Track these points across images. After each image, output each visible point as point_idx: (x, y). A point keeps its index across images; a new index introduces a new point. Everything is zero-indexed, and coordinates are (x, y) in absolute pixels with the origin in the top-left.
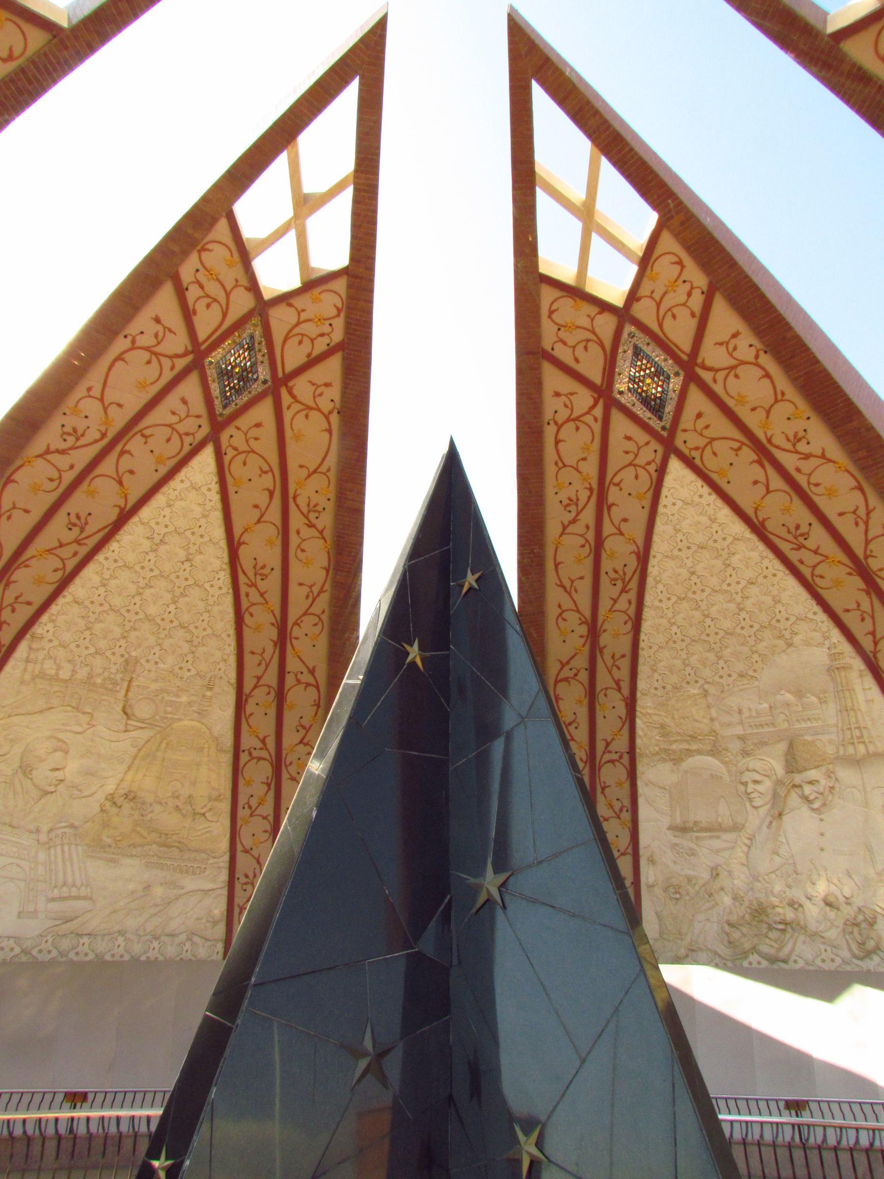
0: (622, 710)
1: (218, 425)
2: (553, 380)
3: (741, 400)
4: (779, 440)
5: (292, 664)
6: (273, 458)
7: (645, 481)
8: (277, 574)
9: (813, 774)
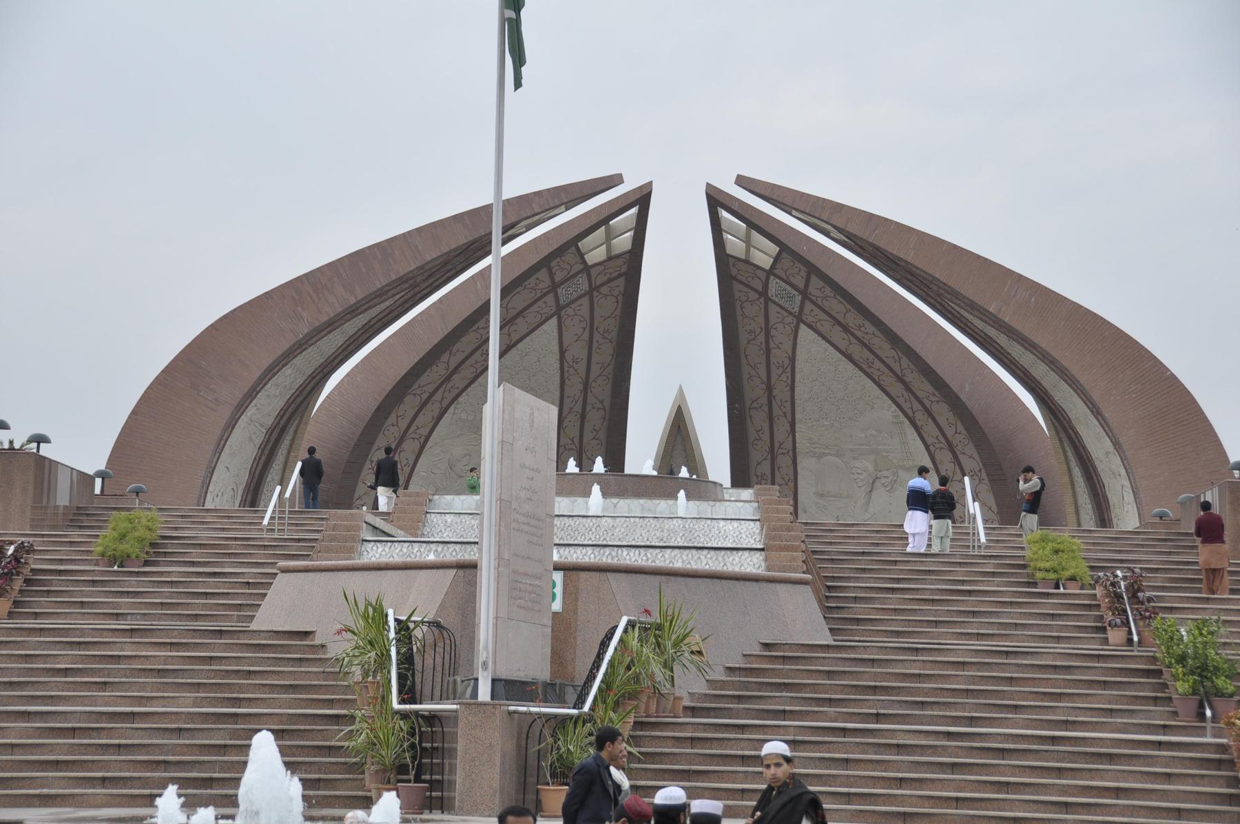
1: (559, 308)
2: (737, 286)
5: (591, 400)
8: (585, 361)
9: (885, 473)
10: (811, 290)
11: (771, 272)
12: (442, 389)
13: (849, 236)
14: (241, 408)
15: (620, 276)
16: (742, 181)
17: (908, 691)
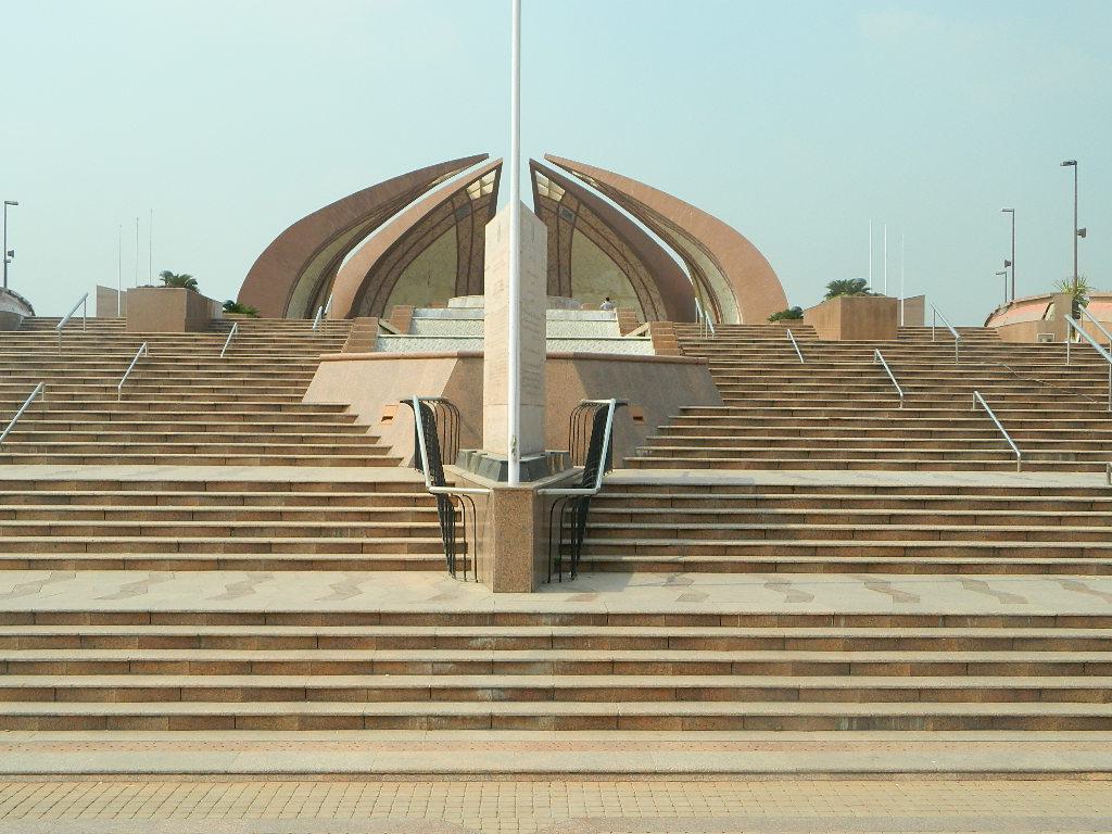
2: (544, 210)
5: (472, 267)
10: (581, 212)
11: (561, 202)
13: (601, 184)
14: (302, 271)
16: (547, 157)
17: (795, 443)
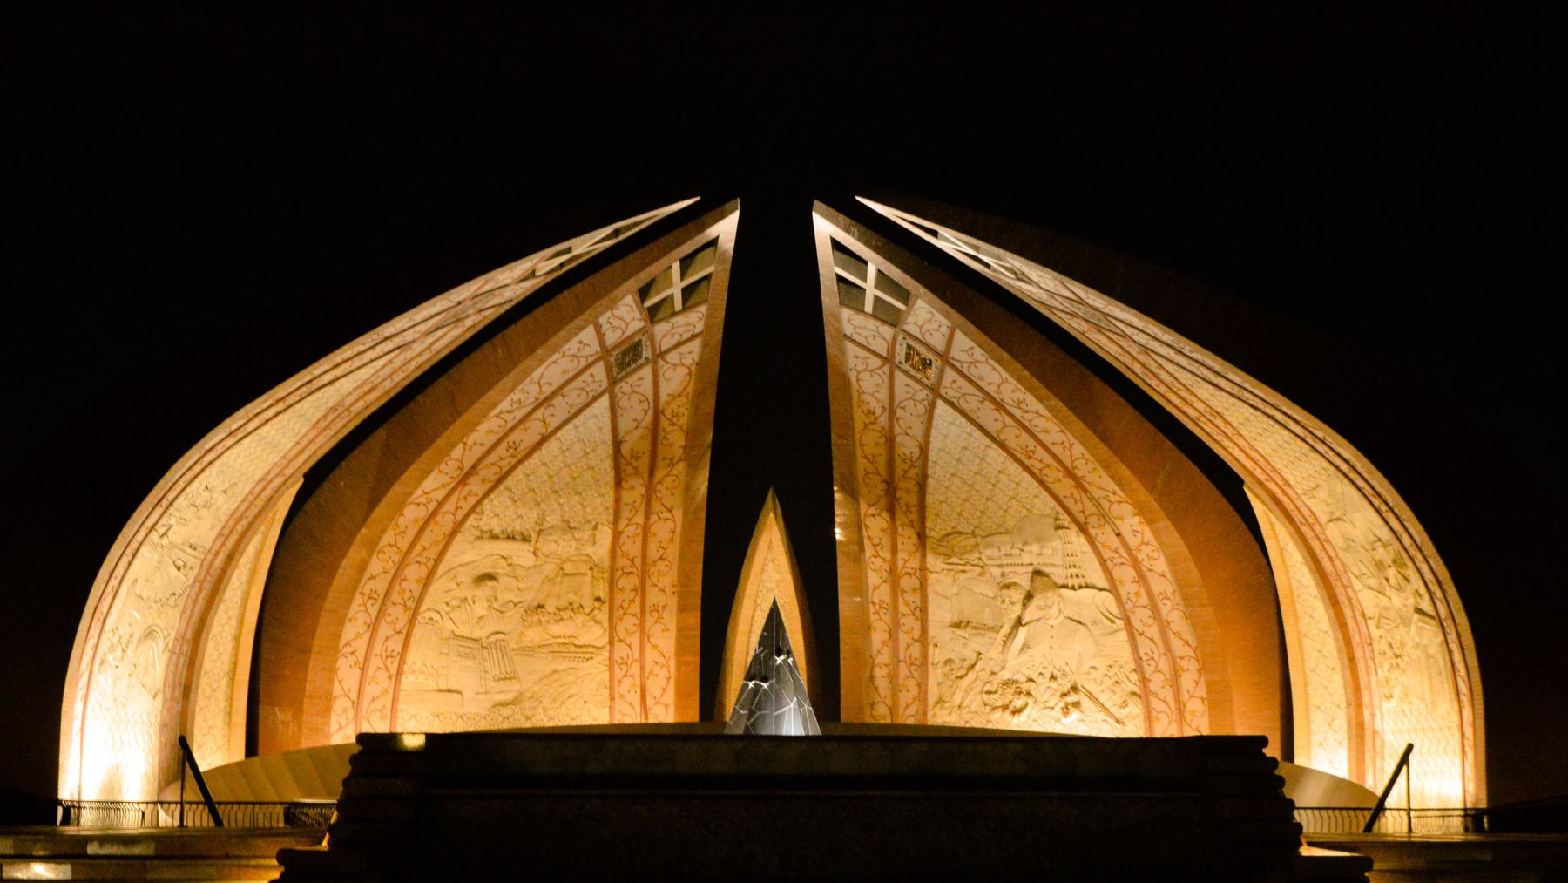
0: (914, 539)
1: (613, 382)
3: (982, 379)
4: (1007, 400)
5: (656, 506)
6: (651, 398)
7: (921, 409)
12: (454, 498)
15: (693, 337)
